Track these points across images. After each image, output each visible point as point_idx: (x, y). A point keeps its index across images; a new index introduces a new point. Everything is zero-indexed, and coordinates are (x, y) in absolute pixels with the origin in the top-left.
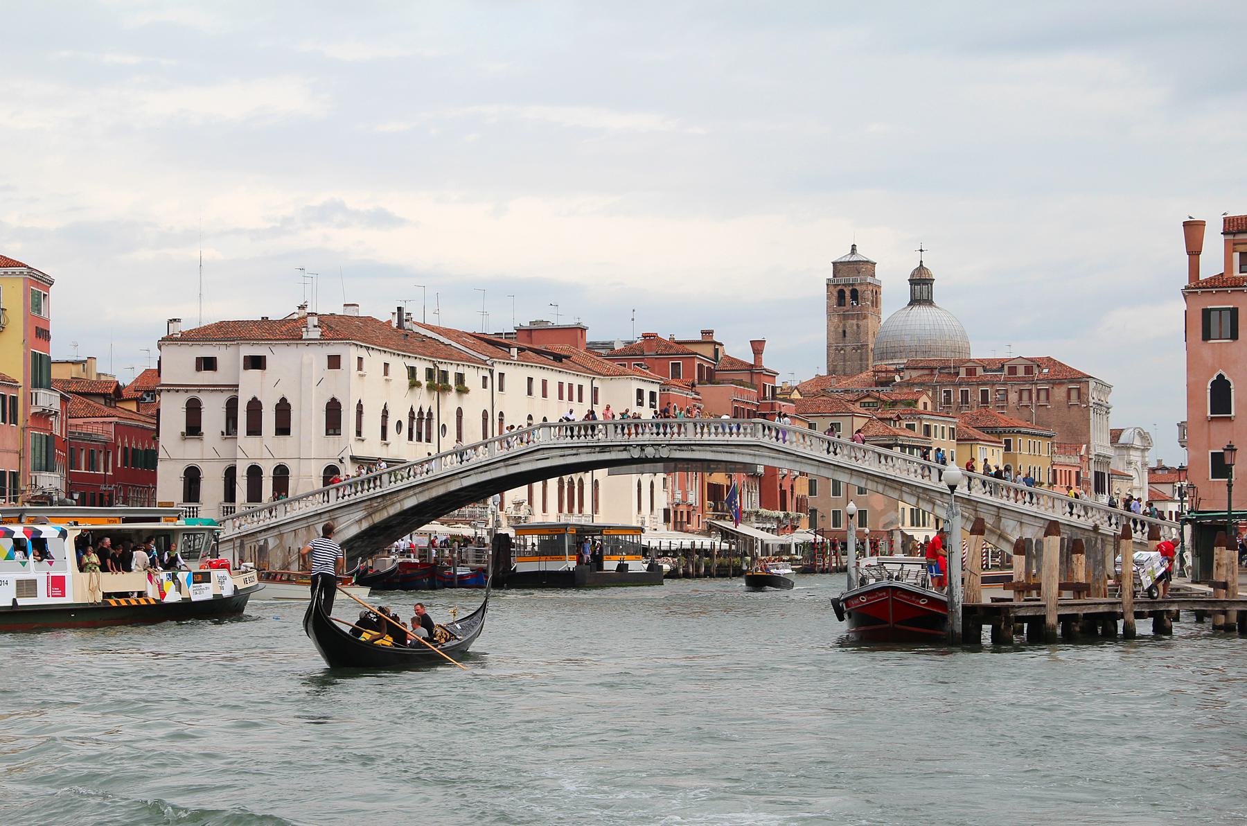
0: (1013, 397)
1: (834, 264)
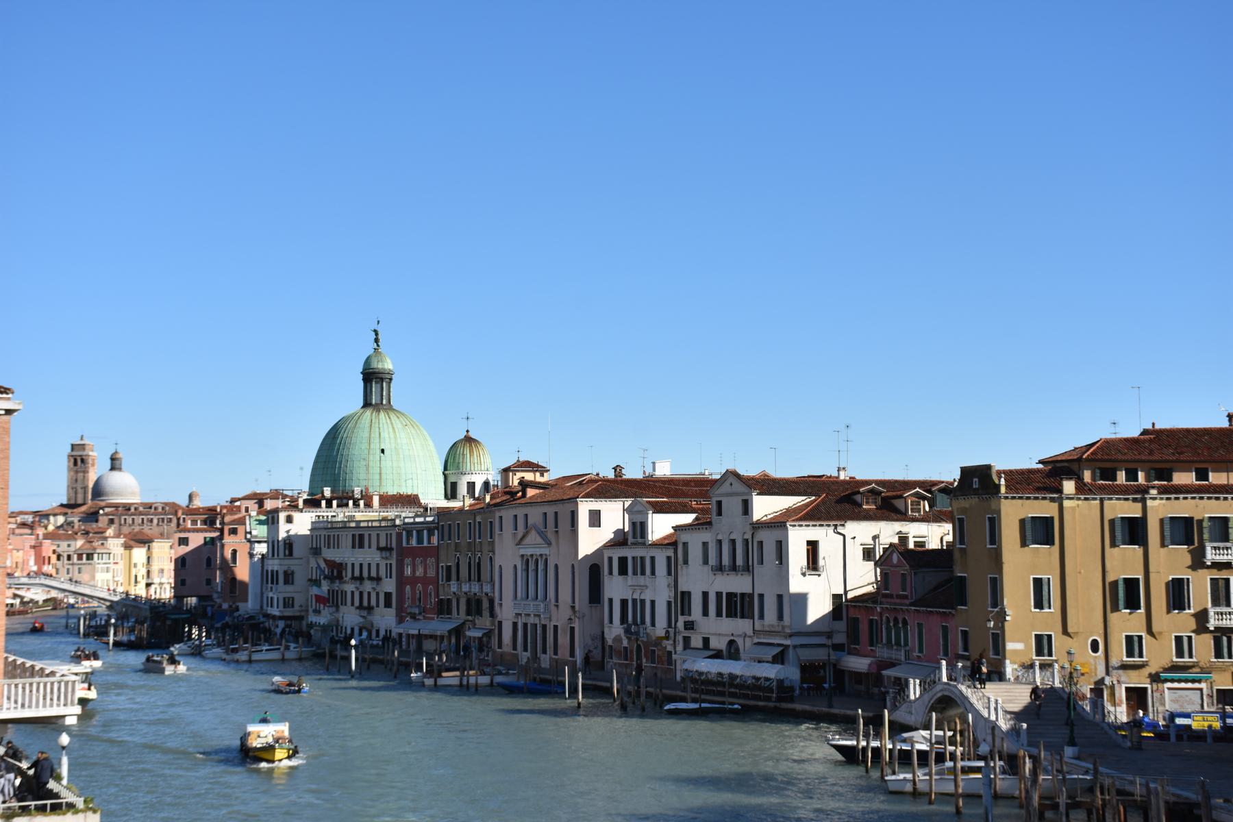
0: (155, 521)
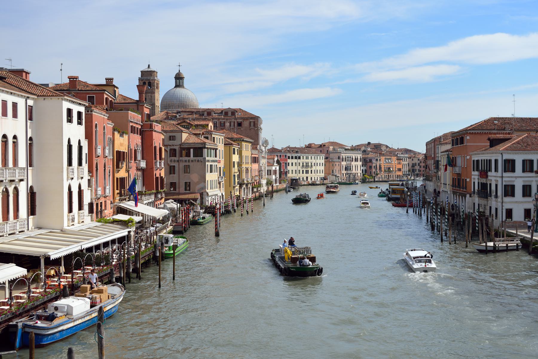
1: (142, 72)
